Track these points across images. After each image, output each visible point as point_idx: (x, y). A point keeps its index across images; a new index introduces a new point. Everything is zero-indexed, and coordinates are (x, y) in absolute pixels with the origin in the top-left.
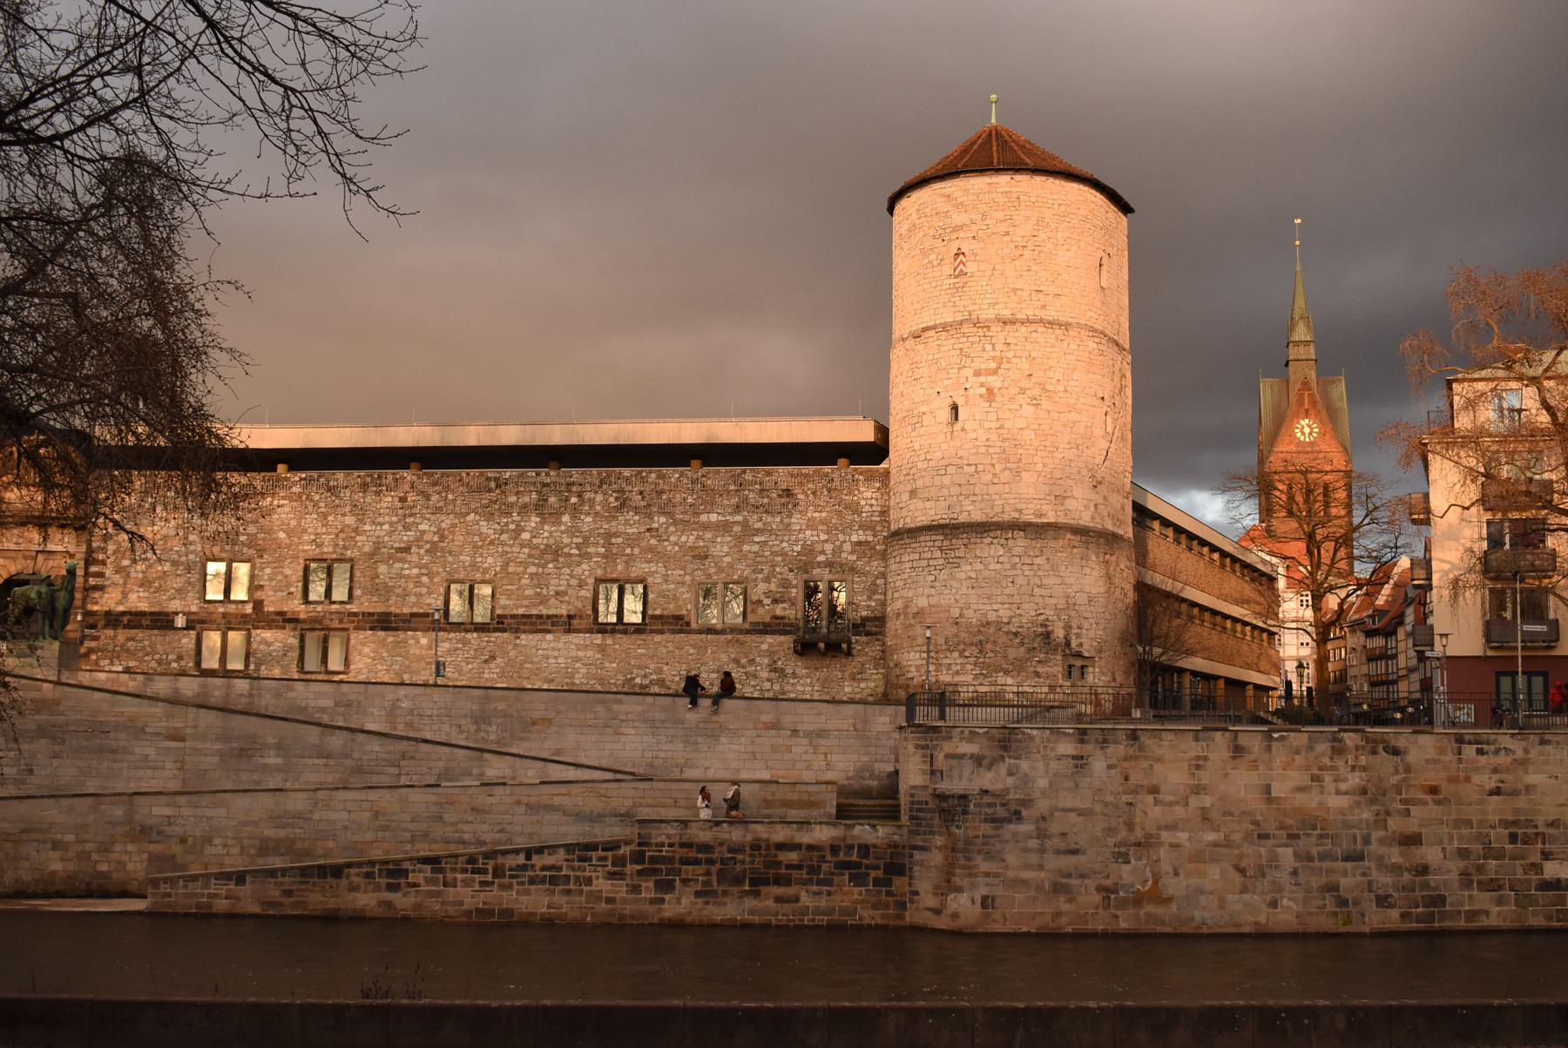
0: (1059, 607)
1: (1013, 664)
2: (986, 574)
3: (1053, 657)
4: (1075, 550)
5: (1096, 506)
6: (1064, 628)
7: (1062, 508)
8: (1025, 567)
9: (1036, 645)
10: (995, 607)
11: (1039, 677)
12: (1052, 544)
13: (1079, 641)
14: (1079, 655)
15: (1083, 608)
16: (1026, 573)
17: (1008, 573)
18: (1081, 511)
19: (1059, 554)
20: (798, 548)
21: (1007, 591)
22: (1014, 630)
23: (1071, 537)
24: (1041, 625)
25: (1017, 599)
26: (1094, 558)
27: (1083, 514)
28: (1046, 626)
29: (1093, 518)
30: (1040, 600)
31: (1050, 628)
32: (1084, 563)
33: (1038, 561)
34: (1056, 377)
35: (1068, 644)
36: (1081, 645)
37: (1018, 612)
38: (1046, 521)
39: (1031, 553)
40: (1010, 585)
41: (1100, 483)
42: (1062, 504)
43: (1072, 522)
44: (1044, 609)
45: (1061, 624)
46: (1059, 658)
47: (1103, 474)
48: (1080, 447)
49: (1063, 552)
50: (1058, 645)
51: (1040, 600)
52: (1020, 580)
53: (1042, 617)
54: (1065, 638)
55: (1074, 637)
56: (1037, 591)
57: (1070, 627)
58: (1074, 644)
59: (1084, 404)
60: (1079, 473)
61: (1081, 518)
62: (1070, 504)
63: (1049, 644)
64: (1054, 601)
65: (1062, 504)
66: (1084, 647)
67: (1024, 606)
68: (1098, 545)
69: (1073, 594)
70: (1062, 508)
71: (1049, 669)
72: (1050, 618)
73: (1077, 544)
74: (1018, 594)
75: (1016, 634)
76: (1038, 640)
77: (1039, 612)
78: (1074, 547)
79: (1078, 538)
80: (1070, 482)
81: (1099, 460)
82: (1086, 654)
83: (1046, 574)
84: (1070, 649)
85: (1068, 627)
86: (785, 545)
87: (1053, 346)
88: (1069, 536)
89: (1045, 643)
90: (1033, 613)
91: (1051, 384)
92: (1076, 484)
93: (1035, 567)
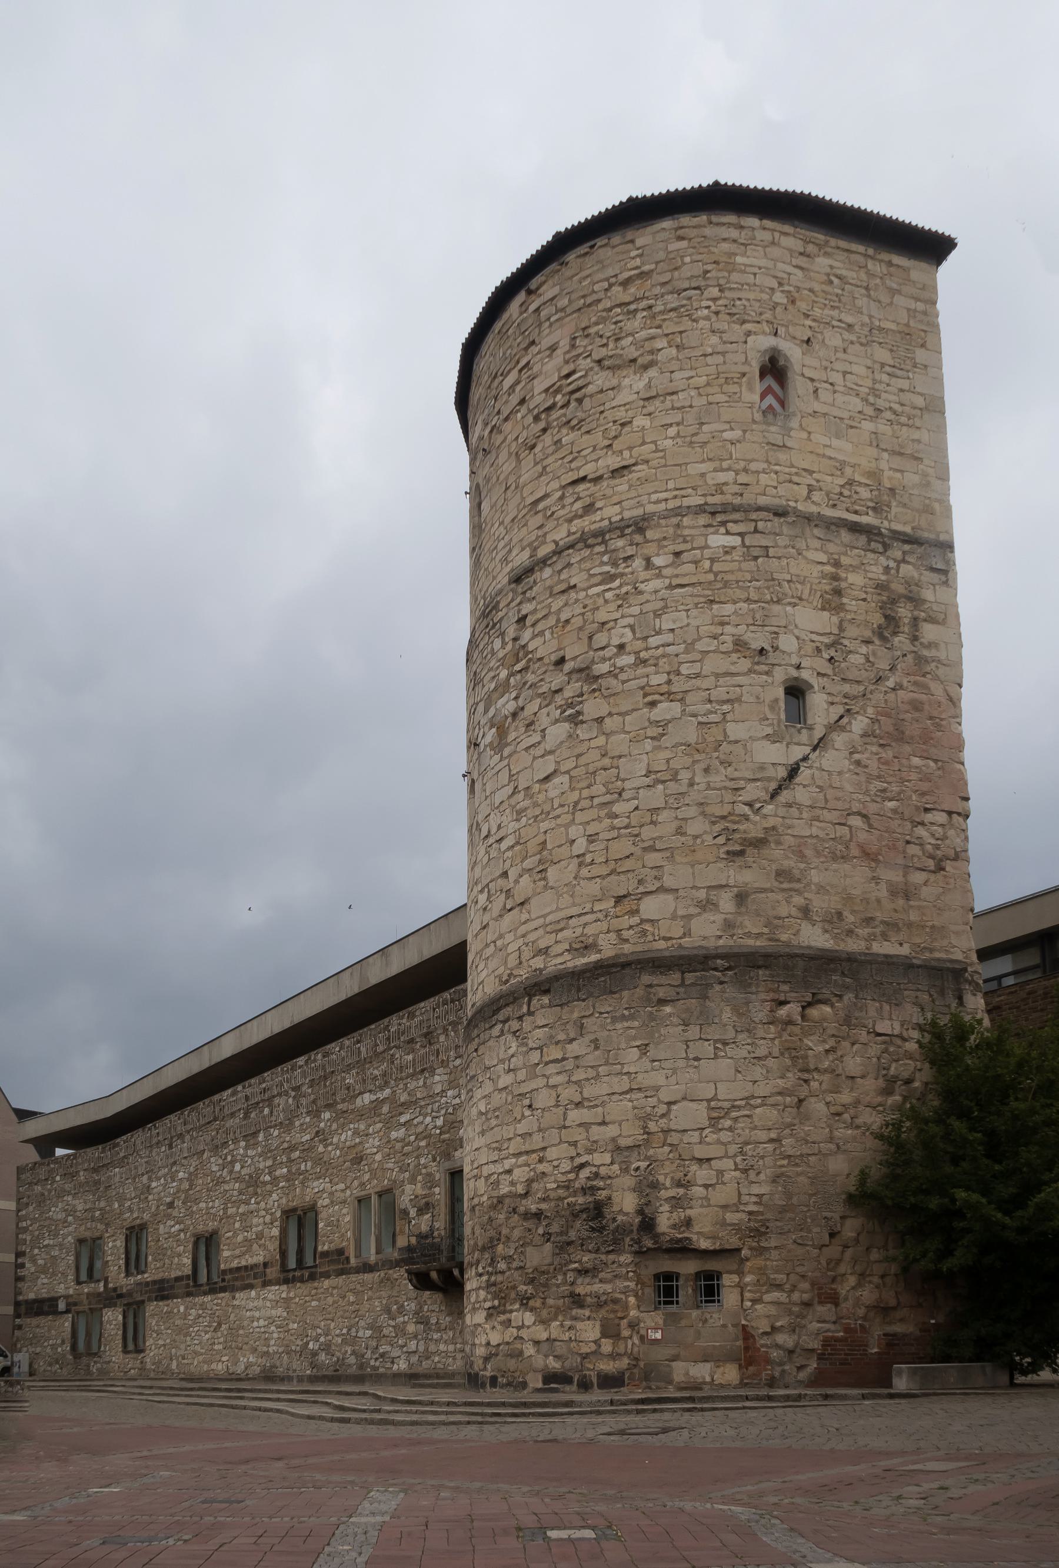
0: (623, 1142)
1: (532, 1281)
2: (498, 1099)
3: (611, 1257)
4: (668, 1009)
5: (741, 898)
6: (637, 1189)
7: (635, 920)
8: (552, 1069)
9: (573, 1235)
10: (507, 1164)
11: (581, 1306)
12: (606, 1005)
13: (681, 1214)
14: (682, 1249)
15: (695, 1137)
16: (552, 1081)
17: (524, 1088)
18: (689, 917)
19: (619, 1026)
20: (440, 1122)
21: (521, 1128)
22: (533, 1208)
23: (654, 980)
24: (584, 1190)
25: (537, 1141)
26: (727, 1015)
27: (695, 924)
28: (593, 1189)
29: (728, 925)
30: (579, 1135)
31: (602, 1195)
32: (694, 1032)
33: (574, 1049)
34: (616, 641)
35: (648, 1224)
36: (688, 1223)
37: (541, 1168)
38: (594, 957)
39: (562, 1036)
40: (527, 1113)
41: (759, 843)
42: (637, 911)
43: (662, 945)
44: (590, 1151)
45: (628, 1181)
46: (626, 1258)
47: (771, 822)
48: (684, 775)
49: (632, 1017)
50: (622, 1230)
51: (579, 1135)
52: (544, 1099)
53: (585, 1173)
54: (640, 1212)
55: (666, 1207)
56: (575, 1116)
57: (655, 1186)
58: (664, 1222)
59: (698, 676)
60: (680, 832)
61: (687, 933)
62: (650, 907)
63: (601, 1229)
64: (611, 1131)
65: (634, 912)
66: (696, 1228)
67: (552, 1153)
68: (744, 986)
69: (662, 1109)
70: (635, 920)
71: (608, 1288)
72: (603, 1171)
73: (671, 993)
74: (540, 1130)
75: (538, 1215)
76: (578, 1224)
77: (579, 1161)
78: (662, 1002)
79: (675, 977)
80: (653, 859)
81: (754, 792)
82: (704, 1244)
83: (591, 1073)
84: (656, 1237)
85: (648, 1186)
86: (428, 1119)
87: (612, 578)
88: (646, 979)
89: (593, 1229)
90: (566, 1166)
91: (604, 660)
92: (671, 858)
93: (569, 1065)
